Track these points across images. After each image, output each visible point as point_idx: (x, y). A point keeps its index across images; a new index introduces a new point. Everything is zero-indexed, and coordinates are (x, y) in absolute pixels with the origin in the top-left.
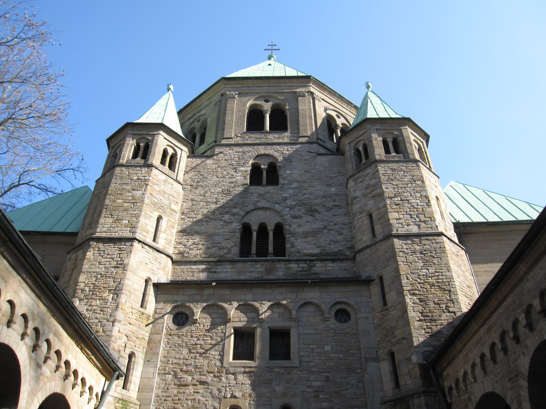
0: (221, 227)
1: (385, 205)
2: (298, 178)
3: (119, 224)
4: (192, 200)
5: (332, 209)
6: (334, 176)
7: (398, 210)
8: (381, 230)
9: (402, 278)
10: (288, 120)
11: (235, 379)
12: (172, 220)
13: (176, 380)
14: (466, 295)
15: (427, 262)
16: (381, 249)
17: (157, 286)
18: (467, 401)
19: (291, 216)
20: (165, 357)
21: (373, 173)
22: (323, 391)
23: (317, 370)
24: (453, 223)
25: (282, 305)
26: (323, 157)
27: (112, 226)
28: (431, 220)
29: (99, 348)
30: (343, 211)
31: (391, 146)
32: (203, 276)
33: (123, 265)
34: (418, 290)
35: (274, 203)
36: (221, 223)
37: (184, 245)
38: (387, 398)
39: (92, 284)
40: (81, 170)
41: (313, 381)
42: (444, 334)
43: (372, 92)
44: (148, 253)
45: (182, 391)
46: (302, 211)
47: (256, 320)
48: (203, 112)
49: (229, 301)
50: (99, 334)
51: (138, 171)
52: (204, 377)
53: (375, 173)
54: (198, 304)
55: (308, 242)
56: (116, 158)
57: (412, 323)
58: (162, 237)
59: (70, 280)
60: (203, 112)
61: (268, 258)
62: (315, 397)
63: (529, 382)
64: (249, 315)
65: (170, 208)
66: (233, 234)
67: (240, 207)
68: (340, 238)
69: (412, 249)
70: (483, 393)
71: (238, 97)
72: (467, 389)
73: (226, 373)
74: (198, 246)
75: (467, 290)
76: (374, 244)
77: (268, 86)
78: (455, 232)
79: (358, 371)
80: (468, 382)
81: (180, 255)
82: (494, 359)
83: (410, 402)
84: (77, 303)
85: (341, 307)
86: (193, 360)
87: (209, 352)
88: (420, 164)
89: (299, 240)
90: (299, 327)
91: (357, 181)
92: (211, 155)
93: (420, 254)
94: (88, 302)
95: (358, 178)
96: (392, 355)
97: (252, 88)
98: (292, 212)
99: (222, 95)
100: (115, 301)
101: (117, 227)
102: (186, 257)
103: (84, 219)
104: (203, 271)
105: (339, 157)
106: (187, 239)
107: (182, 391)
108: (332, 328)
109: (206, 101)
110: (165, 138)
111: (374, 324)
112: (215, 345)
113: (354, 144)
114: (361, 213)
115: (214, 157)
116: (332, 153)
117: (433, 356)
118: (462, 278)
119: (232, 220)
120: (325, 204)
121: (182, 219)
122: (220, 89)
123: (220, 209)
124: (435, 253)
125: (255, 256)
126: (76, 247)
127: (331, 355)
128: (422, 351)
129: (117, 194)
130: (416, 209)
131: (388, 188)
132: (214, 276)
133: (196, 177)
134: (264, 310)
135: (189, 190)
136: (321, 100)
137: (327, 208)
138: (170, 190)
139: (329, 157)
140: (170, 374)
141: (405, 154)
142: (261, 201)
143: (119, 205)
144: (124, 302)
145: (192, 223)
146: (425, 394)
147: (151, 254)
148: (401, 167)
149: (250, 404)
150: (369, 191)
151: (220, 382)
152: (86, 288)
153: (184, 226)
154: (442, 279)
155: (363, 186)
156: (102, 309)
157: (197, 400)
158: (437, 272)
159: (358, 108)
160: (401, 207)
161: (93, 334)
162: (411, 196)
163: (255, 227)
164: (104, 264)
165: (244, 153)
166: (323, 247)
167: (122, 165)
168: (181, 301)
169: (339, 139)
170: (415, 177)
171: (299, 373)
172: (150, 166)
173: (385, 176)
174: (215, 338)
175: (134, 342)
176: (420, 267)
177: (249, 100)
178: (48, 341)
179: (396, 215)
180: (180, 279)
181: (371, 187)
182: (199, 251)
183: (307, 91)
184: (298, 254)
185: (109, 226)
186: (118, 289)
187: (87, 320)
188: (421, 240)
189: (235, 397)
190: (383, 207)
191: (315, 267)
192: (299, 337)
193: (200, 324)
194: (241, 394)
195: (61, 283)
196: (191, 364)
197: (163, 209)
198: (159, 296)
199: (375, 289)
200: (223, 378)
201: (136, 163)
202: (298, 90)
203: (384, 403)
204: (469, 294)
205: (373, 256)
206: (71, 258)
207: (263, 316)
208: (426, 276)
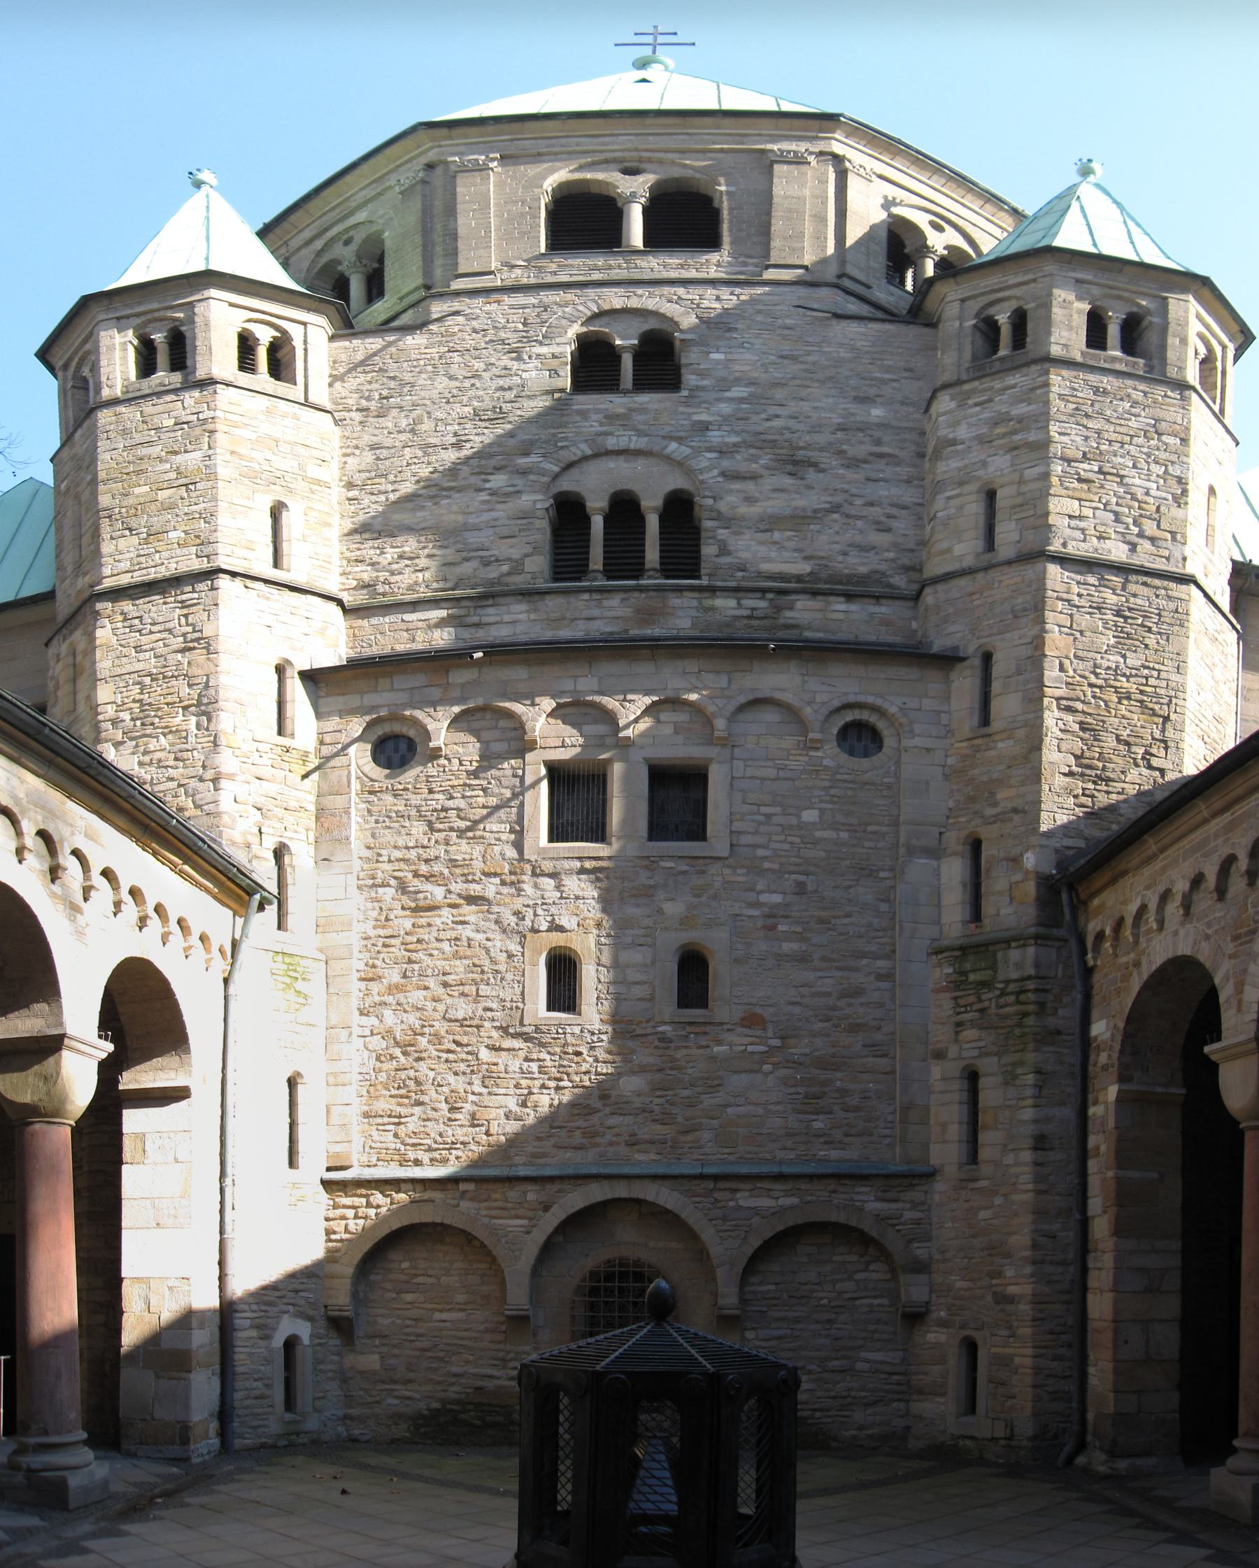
13: (404, 898)
38: (946, 943)
45: (423, 921)
52: (477, 887)
64: (585, 728)
79: (882, 875)
86: (442, 848)
87: (481, 826)
107: (423, 921)
112: (497, 808)
134: (632, 717)
157: (465, 939)
203: (938, 952)
207: (628, 733)
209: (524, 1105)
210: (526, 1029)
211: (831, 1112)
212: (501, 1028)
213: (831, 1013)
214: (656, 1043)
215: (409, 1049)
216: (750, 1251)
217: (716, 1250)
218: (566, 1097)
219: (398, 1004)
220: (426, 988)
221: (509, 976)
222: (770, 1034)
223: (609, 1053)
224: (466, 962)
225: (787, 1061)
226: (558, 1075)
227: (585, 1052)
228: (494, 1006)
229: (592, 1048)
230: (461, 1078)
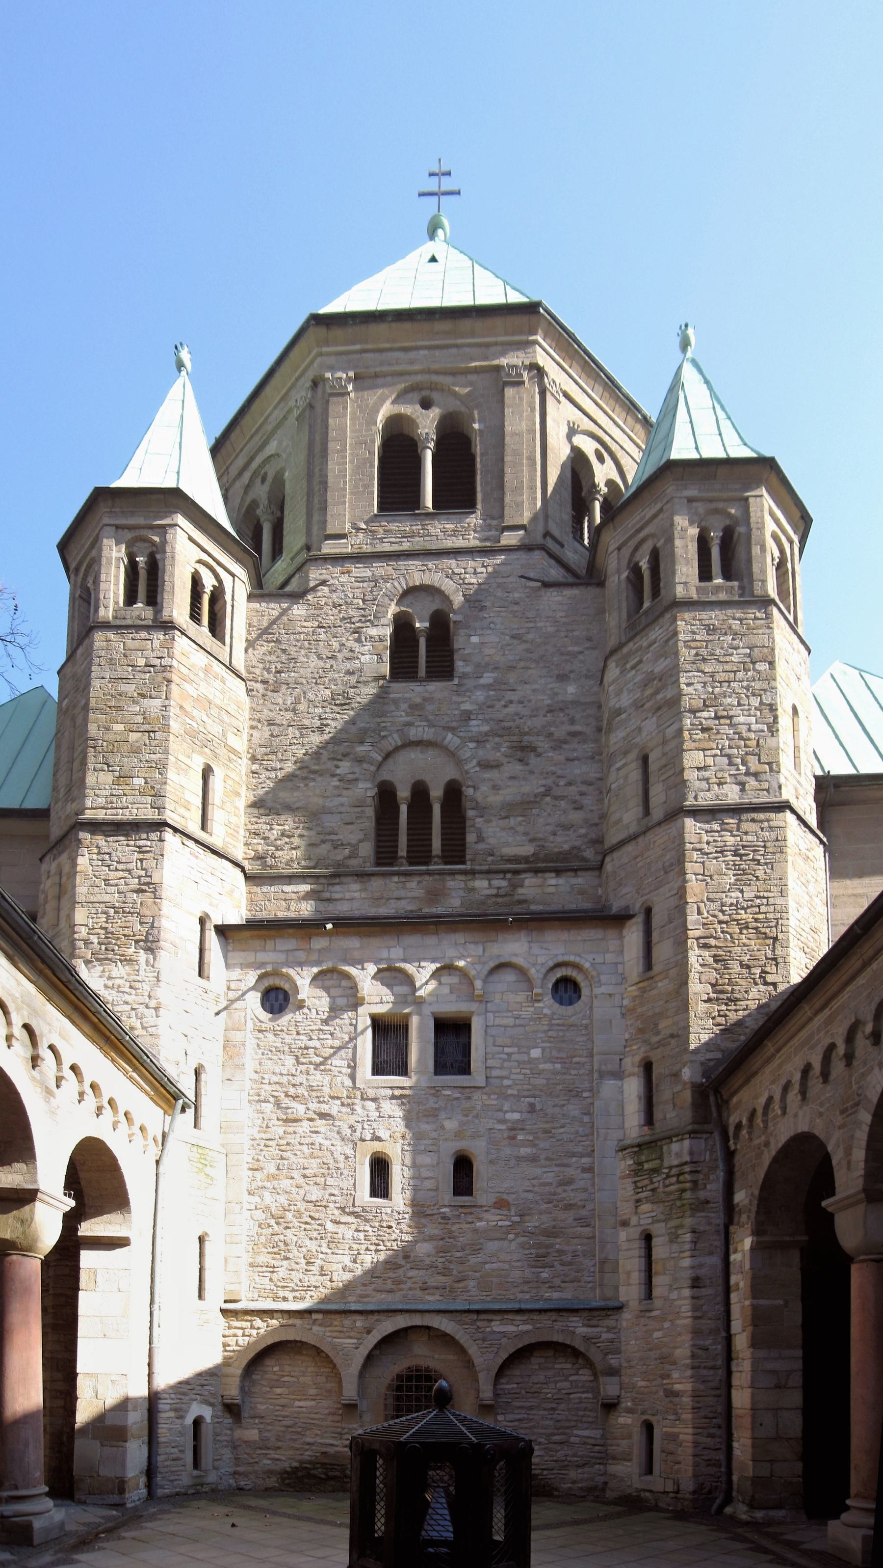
0: (335, 792)
1: (680, 731)
3: (127, 787)
4: (271, 723)
6: (577, 649)
7: (706, 745)
8: (662, 798)
9: (688, 911)
10: (479, 472)
11: (378, 1109)
12: (232, 775)
13: (279, 1111)
14: (806, 948)
15: (744, 874)
16: (657, 844)
17: (222, 931)
18: (762, 1148)
19: (479, 764)
20: (256, 1072)
21: (665, 639)
22: (523, 1129)
23: (515, 1092)
24: (816, 777)
25: (457, 968)
26: (555, 593)
27: (114, 792)
28: (771, 770)
29: (142, 1058)
30: (589, 747)
32: (306, 909)
34: (715, 938)
35: (444, 728)
37: (265, 838)
38: (628, 1142)
39: (101, 928)
40: (20, 640)
42: (747, 1027)
43: (694, 363)
45: (290, 1130)
46: (503, 750)
47: (410, 999)
49: (359, 962)
50: (136, 1033)
51: (145, 642)
52: (323, 1106)
53: (667, 641)
54: (304, 968)
55: (512, 828)
56: (89, 604)
57: (694, 1005)
58: (216, 815)
59: (58, 920)
60: (271, 448)
61: (431, 867)
63: (875, 1115)
64: (397, 989)
65: (226, 745)
66: (359, 809)
68: (576, 817)
69: (719, 844)
70: (792, 1133)
71: (355, 389)
72: (766, 1127)
73: (362, 1099)
74: (292, 839)
75: (810, 938)
76: (644, 833)
78: (816, 800)
79: (585, 1094)
80: (770, 1116)
81: (259, 863)
82: (825, 1075)
83: (665, 1148)
84: (83, 972)
85: (564, 974)
86: (305, 1076)
87: (329, 1062)
88: (775, 611)
89: (494, 824)
90: (488, 1014)
91: (625, 664)
92: (302, 590)
93: (733, 856)
94: (103, 971)
97: (390, 355)
99: (315, 384)
100: (153, 966)
101: (125, 795)
102: (271, 867)
103: (54, 775)
104: (307, 896)
105: (593, 591)
106: (268, 824)
107: (290, 1130)
108: (545, 1015)
109: (275, 408)
110: (191, 539)
111: (621, 1007)
112: (340, 1048)
113: (630, 550)
114: (626, 753)
115: (309, 597)
116: (578, 581)
117: (721, 1069)
118: (805, 911)
119: (356, 776)
120: (552, 729)
121: (253, 773)
122: (308, 360)
123: (330, 746)
124: (762, 853)
125: (404, 861)
126: (53, 847)
127: (541, 1066)
129: (110, 707)
130: (744, 740)
131: (692, 684)
132: (329, 909)
133: (273, 658)
134: (424, 980)
135: (260, 695)
136: (562, 399)
138: (222, 697)
139: (568, 592)
140: (269, 1102)
141: (745, 580)
143: (118, 738)
145: (276, 782)
147: (202, 860)
148: (731, 621)
149: (403, 1150)
150: (649, 691)
151: (353, 1114)
152: (92, 937)
153: (261, 792)
154: (765, 913)
155: (639, 678)
156: (133, 984)
159: (651, 425)
160: (713, 737)
161: (127, 1034)
162: (739, 704)
163: (404, 793)
164: (116, 885)
165: (376, 581)
167: (106, 626)
168: (273, 963)
169: (596, 533)
170: (755, 649)
171: (485, 1097)
172: (168, 626)
173: (691, 648)
174: (339, 1035)
176: (728, 887)
177: (382, 401)
178: (51, 1047)
181: (655, 682)
184: (490, 858)
185: (107, 793)
186: (151, 939)
187: (109, 1006)
188: (740, 821)
189: (379, 1139)
191: (522, 886)
193: (310, 1009)
194: (388, 1133)
195: (43, 926)
196: (301, 1084)
197: (213, 748)
198: (230, 954)
200: (356, 1107)
202: (504, 361)
204: (810, 945)
205: (638, 860)
206: (49, 872)
208: (736, 906)
209: (355, 1261)
210: (356, 1210)
212: (340, 1208)
213: (552, 1197)
214: (440, 1220)
215: (280, 1220)
216: (500, 1361)
217: (478, 1361)
218: (382, 1257)
219: (274, 1188)
220: (292, 1178)
221: (346, 1172)
222: (513, 1213)
223: (410, 1227)
224: (318, 1160)
225: (524, 1232)
226: (377, 1242)
227: (394, 1226)
228: (336, 1192)
229: (399, 1223)
230: (314, 1242)
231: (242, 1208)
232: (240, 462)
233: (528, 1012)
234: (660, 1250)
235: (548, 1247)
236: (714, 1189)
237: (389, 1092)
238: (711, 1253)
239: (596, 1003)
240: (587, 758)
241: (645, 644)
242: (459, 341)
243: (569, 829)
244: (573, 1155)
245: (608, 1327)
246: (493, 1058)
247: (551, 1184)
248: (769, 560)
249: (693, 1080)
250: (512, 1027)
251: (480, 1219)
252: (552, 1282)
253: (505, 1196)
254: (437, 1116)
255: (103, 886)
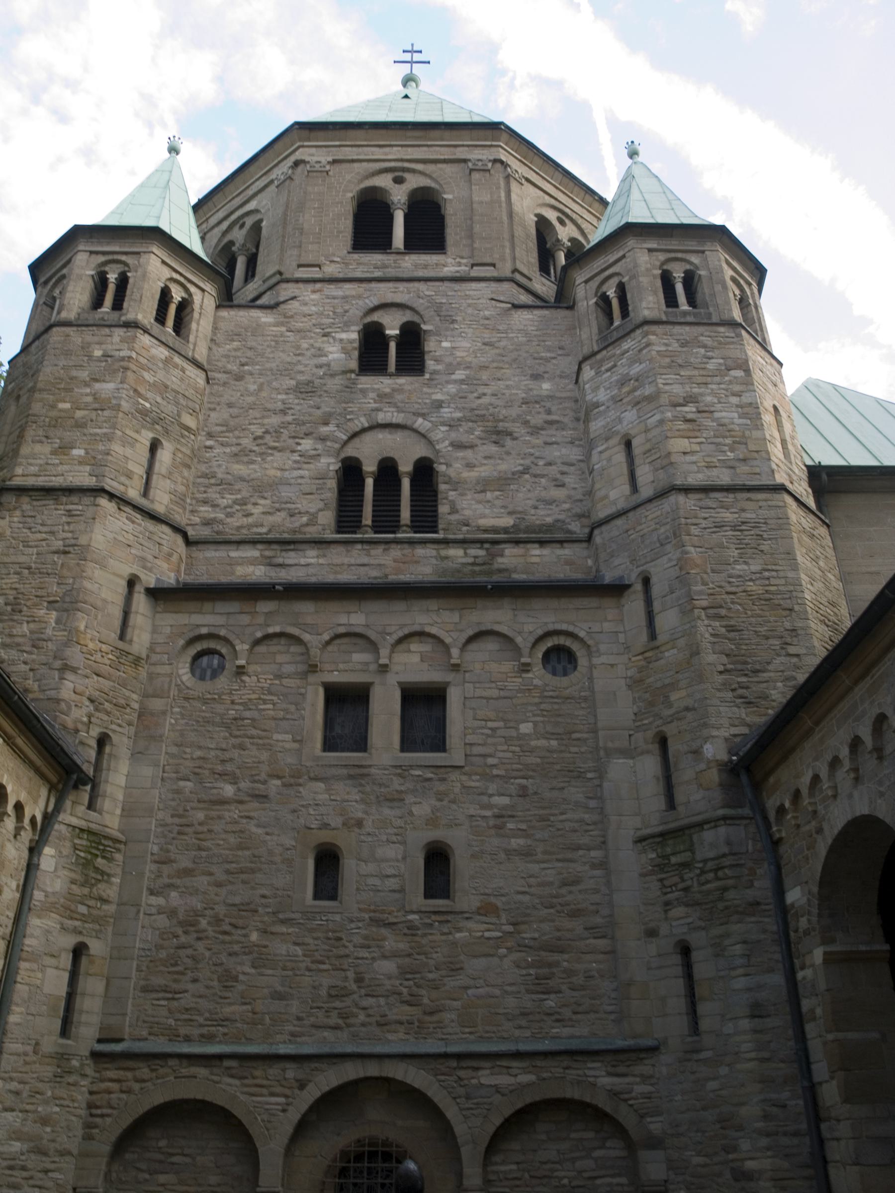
2: (469, 359)
3: (65, 457)
5: (542, 429)
6: (549, 355)
12: (184, 449)
16: (649, 518)
18: (815, 835)
22: (513, 816)
26: (526, 313)
27: (50, 461)
31: (679, 288)
33: (76, 548)
35: (414, 414)
36: (296, 457)
38: (648, 831)
41: (491, 796)
42: (774, 701)
44: (133, 522)
45: (214, 814)
46: (476, 433)
48: (252, 206)
53: (640, 351)
55: (488, 502)
56: (52, 308)
61: (399, 535)
62: (496, 827)
66: (321, 481)
67: (336, 422)
68: (559, 493)
69: (717, 520)
75: (829, 611)
76: (635, 508)
77: (402, 146)
78: (811, 485)
79: (589, 775)
83: (695, 837)
85: (556, 643)
88: (743, 333)
89: (469, 497)
90: (467, 685)
95: (602, 361)
96: (663, 742)
97: (365, 149)
98: (453, 435)
105: (561, 314)
107: (214, 814)
108: (535, 686)
110: (163, 262)
117: (749, 746)
118: (819, 585)
119: (319, 452)
120: (528, 418)
125: (369, 530)
127: (533, 743)
128: (727, 734)
129: (59, 389)
133: (239, 354)
137: (531, 427)
139: (537, 312)
142: (385, 409)
143: (63, 414)
144: (82, 628)
146: (728, 822)
147: (140, 525)
150: (626, 389)
155: (615, 378)
158: (768, 570)
163: (370, 467)
164: (36, 546)
166: (520, 512)
167: (67, 324)
171: (464, 778)
175: (108, 713)
179: (682, 444)
180: (204, 579)
181: (632, 382)
182: (245, 519)
183: (492, 158)
184: (465, 528)
190: (657, 426)
191: (502, 556)
192: (464, 704)
196: (231, 760)
197: (165, 425)
199: (634, 604)
201: (99, 319)
204: (831, 618)
205: (629, 533)
211: (560, 992)
214: (406, 931)
216: (491, 1129)
217: (460, 1129)
222: (504, 921)
225: (519, 946)
231: (138, 911)
232: (221, 214)
233: (515, 683)
234: (703, 968)
235: (550, 965)
236: (762, 886)
237: (345, 771)
238: (771, 970)
239: (596, 673)
240: (567, 443)
241: (618, 352)
242: (429, 143)
243: (551, 504)
244: (578, 848)
245: (642, 1076)
246: (474, 733)
247: (551, 884)
248: (731, 295)
249: (718, 758)
250: (497, 699)
251: (459, 930)
252: (558, 1013)
253: (493, 900)
254: (404, 800)
255: (21, 547)
